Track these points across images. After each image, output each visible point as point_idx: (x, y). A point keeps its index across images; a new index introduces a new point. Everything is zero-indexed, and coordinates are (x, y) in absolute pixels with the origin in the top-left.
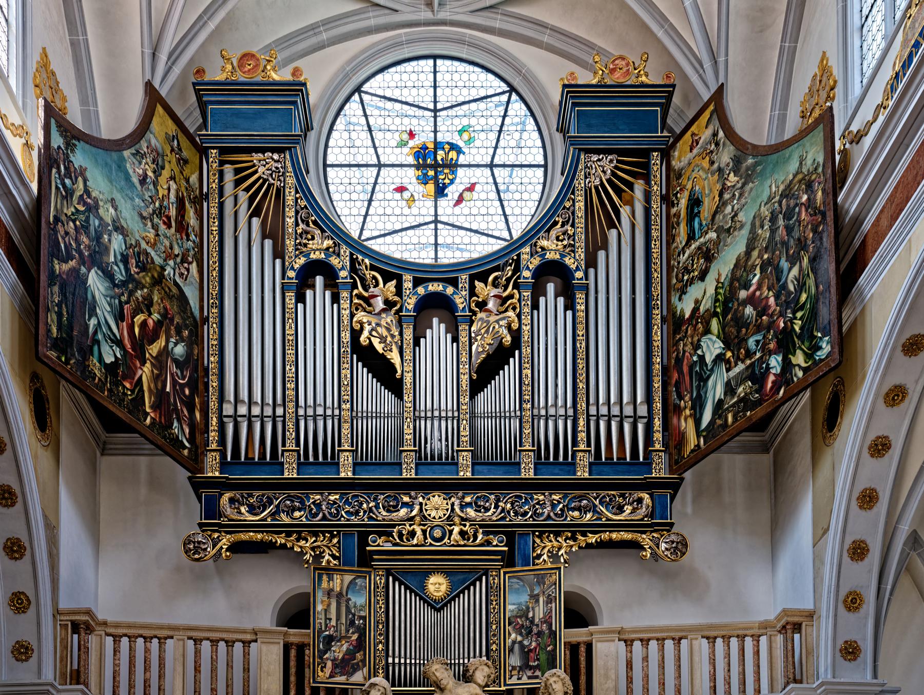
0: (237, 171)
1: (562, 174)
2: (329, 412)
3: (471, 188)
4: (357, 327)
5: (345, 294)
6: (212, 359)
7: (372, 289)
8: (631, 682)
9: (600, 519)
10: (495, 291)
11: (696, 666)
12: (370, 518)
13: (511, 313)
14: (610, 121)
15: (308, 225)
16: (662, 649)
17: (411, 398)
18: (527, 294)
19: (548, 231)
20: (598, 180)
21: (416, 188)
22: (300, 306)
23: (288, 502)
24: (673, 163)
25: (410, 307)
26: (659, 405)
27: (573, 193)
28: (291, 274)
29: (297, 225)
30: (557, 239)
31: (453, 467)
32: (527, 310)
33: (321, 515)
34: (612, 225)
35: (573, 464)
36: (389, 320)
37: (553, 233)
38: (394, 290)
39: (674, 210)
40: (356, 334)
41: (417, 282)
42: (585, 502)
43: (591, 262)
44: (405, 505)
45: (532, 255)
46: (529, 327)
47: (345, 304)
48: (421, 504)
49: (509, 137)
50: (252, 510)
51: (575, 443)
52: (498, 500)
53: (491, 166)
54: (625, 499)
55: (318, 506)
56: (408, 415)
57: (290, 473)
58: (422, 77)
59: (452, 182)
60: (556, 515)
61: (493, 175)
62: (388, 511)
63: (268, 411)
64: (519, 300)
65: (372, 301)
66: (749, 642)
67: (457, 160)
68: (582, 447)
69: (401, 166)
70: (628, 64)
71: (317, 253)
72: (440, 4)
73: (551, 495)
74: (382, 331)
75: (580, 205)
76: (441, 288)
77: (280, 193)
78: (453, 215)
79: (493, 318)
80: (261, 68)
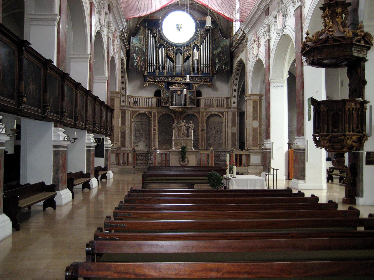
16: (210, 100)
18: (192, 49)
40: (167, 54)
41: (176, 47)
43: (201, 44)
44: (174, 79)
50: (152, 79)
55: (162, 79)
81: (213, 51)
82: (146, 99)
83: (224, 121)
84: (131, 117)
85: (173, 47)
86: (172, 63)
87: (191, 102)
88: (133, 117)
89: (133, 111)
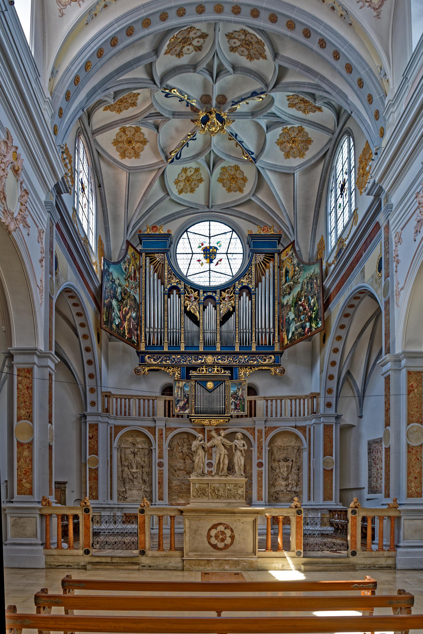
0: (150, 259)
2: (177, 331)
3: (221, 260)
4: (186, 305)
5: (182, 296)
11: (286, 407)
12: (190, 363)
13: (232, 302)
16: (276, 402)
18: (237, 295)
19: (244, 277)
21: (204, 261)
22: (169, 299)
24: (281, 258)
25: (202, 300)
26: (277, 329)
28: (166, 290)
29: (168, 275)
30: (247, 279)
31: (215, 348)
32: (237, 300)
34: (263, 275)
35: (251, 347)
37: (245, 277)
39: (281, 272)
41: (204, 292)
43: (257, 286)
44: (200, 359)
47: (182, 299)
50: (154, 360)
51: (251, 341)
52: (228, 357)
56: (201, 332)
57: (166, 349)
59: (215, 258)
61: (227, 256)
62: (195, 361)
63: (159, 330)
69: (199, 253)
74: (194, 307)
75: (253, 269)
76: (211, 294)
77: (163, 265)
79: (227, 303)
81: (282, 298)
82: (142, 401)
83: (306, 445)
84: (111, 438)
85: (199, 294)
86: (195, 327)
87: (236, 405)
88: (115, 438)
89: (116, 427)
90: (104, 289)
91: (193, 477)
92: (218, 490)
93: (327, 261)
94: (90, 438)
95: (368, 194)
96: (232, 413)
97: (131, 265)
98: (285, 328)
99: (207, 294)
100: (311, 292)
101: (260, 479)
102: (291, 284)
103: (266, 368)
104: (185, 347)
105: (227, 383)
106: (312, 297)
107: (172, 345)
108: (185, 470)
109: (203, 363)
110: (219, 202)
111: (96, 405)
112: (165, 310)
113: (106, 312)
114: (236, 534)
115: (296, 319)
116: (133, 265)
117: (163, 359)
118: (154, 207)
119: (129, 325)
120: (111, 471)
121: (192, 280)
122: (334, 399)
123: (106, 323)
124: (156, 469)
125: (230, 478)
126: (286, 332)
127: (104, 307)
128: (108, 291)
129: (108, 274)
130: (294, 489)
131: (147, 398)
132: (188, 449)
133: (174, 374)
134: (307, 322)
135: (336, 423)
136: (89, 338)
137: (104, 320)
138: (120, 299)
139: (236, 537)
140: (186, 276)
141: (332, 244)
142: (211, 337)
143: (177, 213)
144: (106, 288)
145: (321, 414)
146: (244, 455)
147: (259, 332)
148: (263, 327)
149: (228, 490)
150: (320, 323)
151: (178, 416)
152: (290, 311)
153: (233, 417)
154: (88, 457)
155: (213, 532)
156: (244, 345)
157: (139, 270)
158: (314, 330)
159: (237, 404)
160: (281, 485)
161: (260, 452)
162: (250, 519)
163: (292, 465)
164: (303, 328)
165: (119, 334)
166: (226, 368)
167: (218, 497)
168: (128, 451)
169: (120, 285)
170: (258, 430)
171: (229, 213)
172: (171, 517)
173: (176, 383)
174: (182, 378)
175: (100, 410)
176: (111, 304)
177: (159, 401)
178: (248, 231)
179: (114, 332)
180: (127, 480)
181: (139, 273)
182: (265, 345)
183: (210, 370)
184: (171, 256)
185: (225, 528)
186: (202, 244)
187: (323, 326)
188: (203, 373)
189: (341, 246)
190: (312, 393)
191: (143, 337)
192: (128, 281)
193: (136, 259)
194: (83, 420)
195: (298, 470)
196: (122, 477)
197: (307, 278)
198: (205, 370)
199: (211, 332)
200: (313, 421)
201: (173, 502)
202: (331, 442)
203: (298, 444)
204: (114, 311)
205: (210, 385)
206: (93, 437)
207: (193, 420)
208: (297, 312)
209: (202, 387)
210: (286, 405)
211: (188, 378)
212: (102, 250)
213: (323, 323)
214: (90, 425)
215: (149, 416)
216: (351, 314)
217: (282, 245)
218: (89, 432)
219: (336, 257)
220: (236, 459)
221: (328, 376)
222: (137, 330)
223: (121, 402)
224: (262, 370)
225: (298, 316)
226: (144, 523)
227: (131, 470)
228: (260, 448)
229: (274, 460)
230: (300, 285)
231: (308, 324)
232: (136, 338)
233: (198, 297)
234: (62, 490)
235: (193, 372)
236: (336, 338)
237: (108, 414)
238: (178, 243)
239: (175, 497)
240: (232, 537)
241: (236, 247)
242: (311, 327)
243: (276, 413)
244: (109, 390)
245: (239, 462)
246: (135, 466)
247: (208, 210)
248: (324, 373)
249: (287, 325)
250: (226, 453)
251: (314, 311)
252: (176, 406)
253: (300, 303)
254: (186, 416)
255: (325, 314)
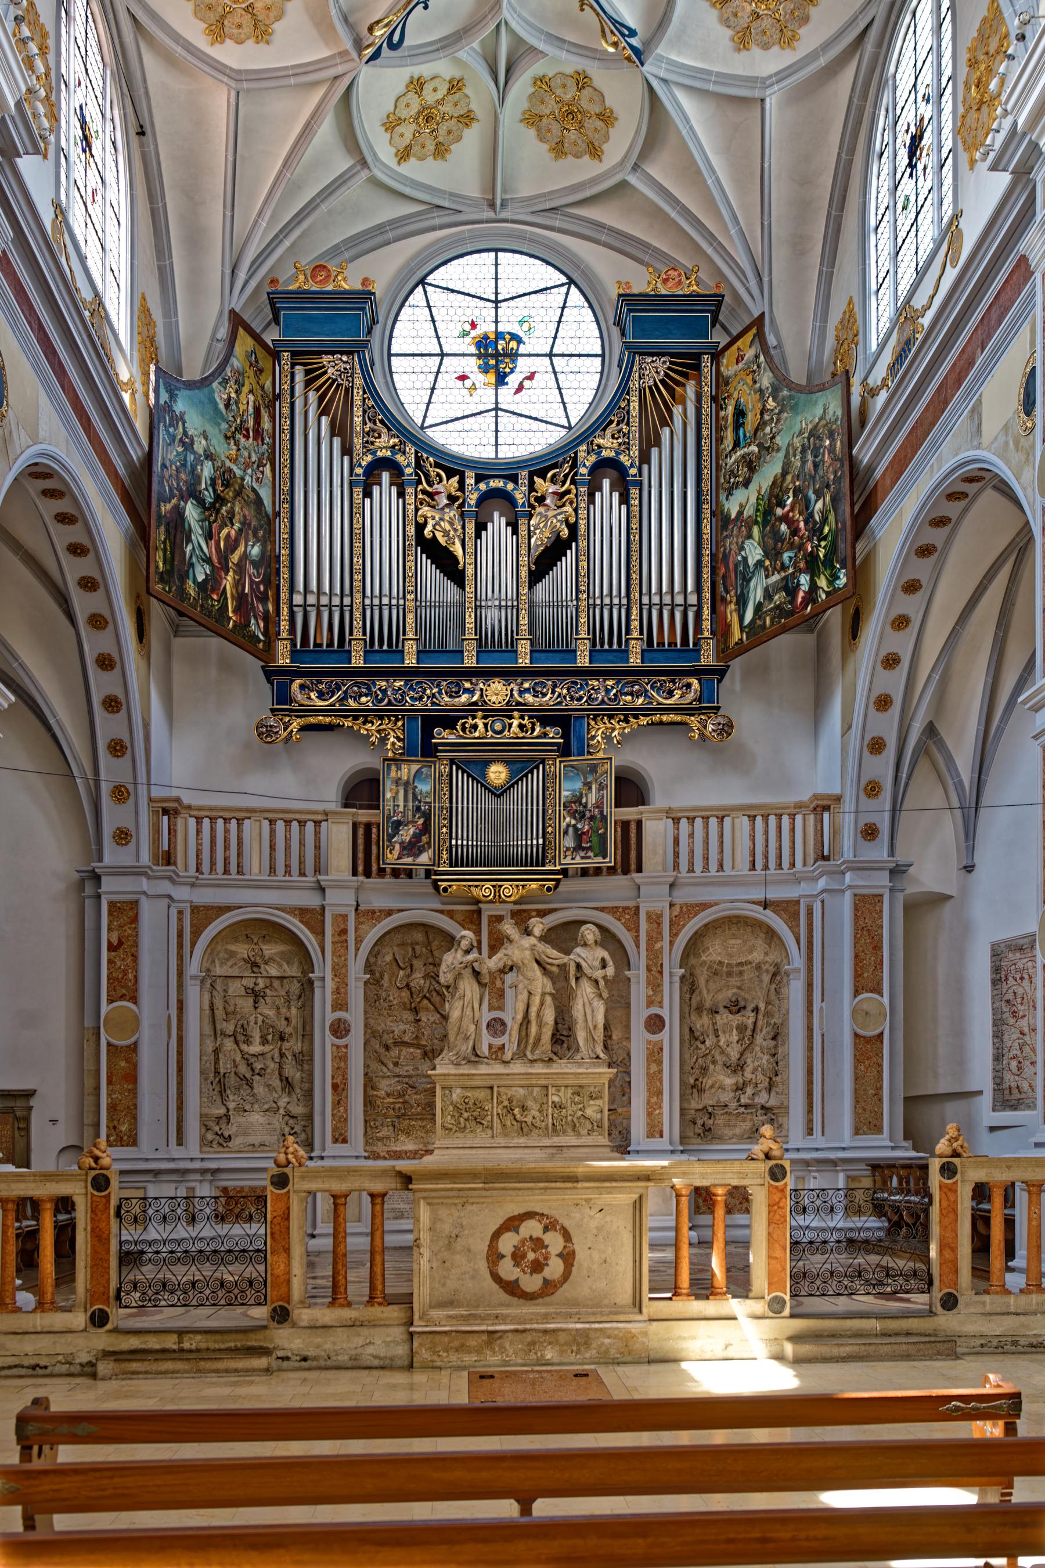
0: (307, 372)
1: (620, 366)
2: (394, 602)
3: (531, 377)
4: (421, 520)
5: (410, 490)
6: (283, 552)
7: (436, 486)
8: (678, 857)
9: (651, 703)
10: (552, 489)
12: (433, 704)
13: (568, 509)
14: (664, 326)
15: (375, 423)
17: (473, 589)
18: (583, 490)
19: (604, 430)
20: (652, 380)
21: (479, 378)
22: (367, 501)
23: (356, 688)
24: (722, 369)
25: (472, 502)
26: (708, 595)
27: (628, 394)
28: (359, 471)
29: (365, 423)
30: (613, 437)
31: (513, 655)
32: (583, 505)
33: (386, 701)
34: (664, 423)
35: (627, 651)
36: (452, 515)
37: (609, 432)
38: (457, 485)
39: (722, 414)
40: (420, 528)
41: (479, 479)
42: (637, 687)
43: (645, 458)
44: (466, 691)
45: (588, 453)
46: (585, 521)
47: (410, 499)
48: (482, 690)
49: (569, 327)
50: (321, 696)
51: (628, 632)
52: (555, 686)
53: (551, 355)
54: (675, 683)
56: (470, 605)
57: (357, 661)
58: (484, 269)
60: (609, 699)
61: (552, 364)
62: (451, 696)
63: (336, 601)
64: (576, 495)
65: (436, 497)
66: (785, 819)
67: (517, 350)
68: (635, 635)
70: (680, 275)
71: (384, 451)
72: (502, 205)
73: (605, 680)
74: (446, 525)
75: (635, 405)
76: (501, 484)
77: (349, 391)
78: (513, 402)
79: (550, 513)
80: (333, 277)
81: (723, 497)
82: (280, 826)
84: (180, 946)
86: (451, 591)
87: (579, 836)
88: (193, 944)
89: (195, 909)
90: (157, 467)
91: (443, 1067)
92: (524, 1108)
93: (866, 379)
94: (111, 947)
95: (994, 168)
96: (568, 860)
97: (245, 389)
98: (732, 593)
99: (487, 484)
100: (813, 478)
101: (654, 1068)
102: (752, 453)
103: (673, 717)
104: (419, 652)
105: (550, 768)
106: (819, 494)
107: (376, 647)
108: (418, 1046)
109: (475, 704)
110: (525, 190)
111: (134, 840)
112: (355, 535)
113: (164, 543)
114: (579, 1246)
115: (767, 563)
116: (251, 391)
117: (350, 692)
118: (318, 205)
119: (238, 583)
120: (180, 1053)
121: (441, 441)
122: (887, 816)
123: (163, 578)
124: (324, 1044)
125: (562, 1067)
126: (737, 603)
127: (158, 527)
128: (171, 476)
129: (171, 419)
130: (762, 1099)
131: (298, 816)
132: (426, 977)
133: (383, 740)
134: (801, 571)
135: (892, 890)
136: (110, 627)
137: (157, 567)
138: (209, 500)
139: (581, 1255)
140: (422, 428)
141: (881, 325)
142: (500, 621)
143: (391, 222)
144: (164, 466)
145: (844, 862)
146: (605, 995)
147: (650, 605)
148: (664, 590)
149: (555, 1105)
150: (842, 574)
151: (396, 873)
152: (750, 536)
153: (570, 873)
154: (105, 1008)
155: (507, 1243)
156: (606, 647)
157: (271, 406)
158: (824, 596)
159: (584, 833)
160: (722, 1087)
161: (655, 985)
162: (623, 1197)
163: (755, 1023)
164: (790, 588)
165: (206, 611)
166: (547, 719)
167: (523, 1129)
168: (235, 988)
169: (209, 456)
170: (647, 913)
171: (557, 224)
172: (372, 1196)
173: (389, 766)
174: (408, 752)
175: (145, 858)
176: (179, 514)
177: (334, 828)
178: (620, 283)
179: (191, 605)
180: (232, 1080)
181: (273, 418)
182: (670, 644)
183: (498, 726)
184: (373, 364)
185: (546, 1229)
186: (473, 325)
187: (850, 586)
188: (477, 734)
189: (908, 332)
190: (815, 797)
191: (283, 623)
192: (237, 444)
193: (261, 371)
194: (89, 890)
195: (774, 1038)
196: (217, 1072)
197: (801, 433)
198: (481, 726)
199: (500, 607)
200: (822, 883)
201: (380, 1148)
202: (878, 948)
203: (774, 957)
204: (189, 540)
205: (497, 773)
206: (120, 943)
207: (444, 884)
208: (770, 542)
209: (474, 779)
210: (738, 834)
211: (429, 751)
212: (152, 340)
213: (852, 575)
214: (112, 905)
215: (302, 874)
216: (939, 547)
217: (724, 327)
218: (110, 929)
219: (893, 368)
220: (580, 1007)
221: (866, 742)
222: (264, 599)
223: (213, 830)
224: (661, 723)
225: (772, 552)
226: (287, 1217)
227: (244, 1047)
228: (655, 970)
229: (699, 1009)
230: (781, 455)
231: (804, 580)
232: (262, 625)
233: (459, 494)
234: (18, 1119)
235: (444, 734)
236: (893, 622)
237: (173, 868)
238: (395, 320)
239: (384, 1132)
240: (568, 1257)
241: (579, 334)
242: (814, 587)
243: (706, 859)
244: (175, 793)
245: (589, 1017)
246: (257, 1039)
247: (491, 215)
248: (855, 732)
249: (739, 582)
250: (549, 988)
251: (825, 538)
252: (389, 841)
253: (779, 511)
254: (422, 874)
255: (859, 547)
